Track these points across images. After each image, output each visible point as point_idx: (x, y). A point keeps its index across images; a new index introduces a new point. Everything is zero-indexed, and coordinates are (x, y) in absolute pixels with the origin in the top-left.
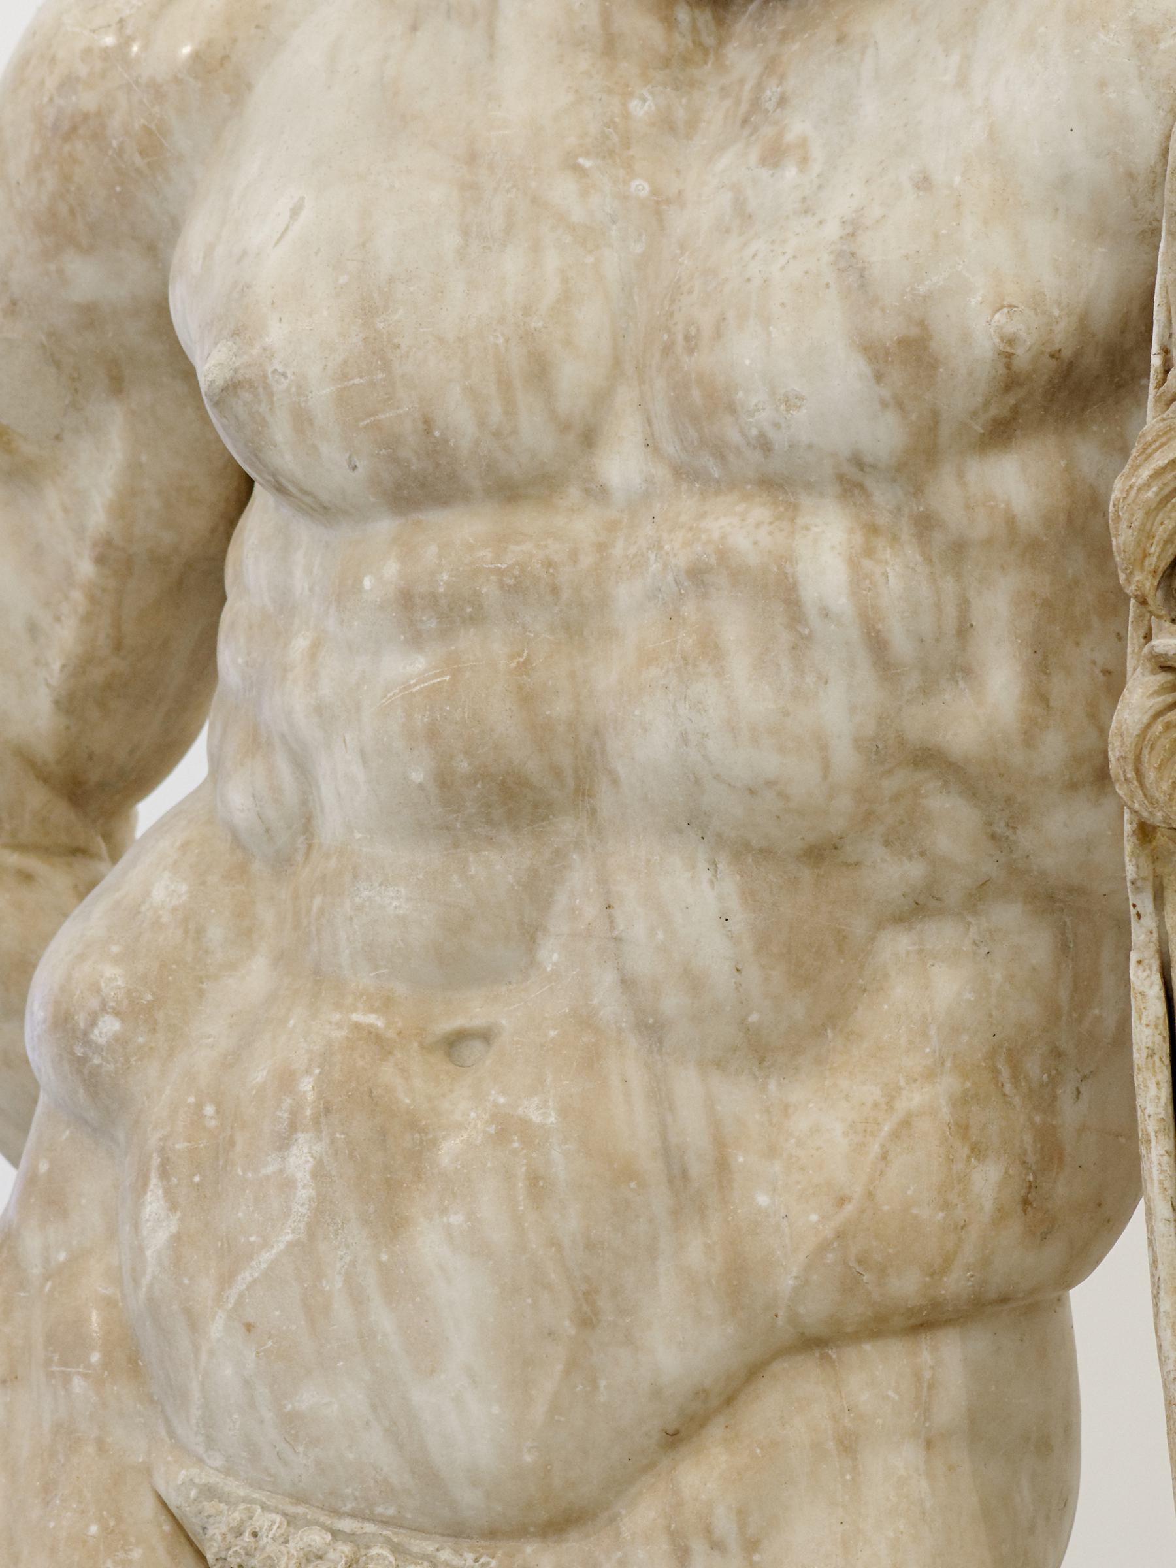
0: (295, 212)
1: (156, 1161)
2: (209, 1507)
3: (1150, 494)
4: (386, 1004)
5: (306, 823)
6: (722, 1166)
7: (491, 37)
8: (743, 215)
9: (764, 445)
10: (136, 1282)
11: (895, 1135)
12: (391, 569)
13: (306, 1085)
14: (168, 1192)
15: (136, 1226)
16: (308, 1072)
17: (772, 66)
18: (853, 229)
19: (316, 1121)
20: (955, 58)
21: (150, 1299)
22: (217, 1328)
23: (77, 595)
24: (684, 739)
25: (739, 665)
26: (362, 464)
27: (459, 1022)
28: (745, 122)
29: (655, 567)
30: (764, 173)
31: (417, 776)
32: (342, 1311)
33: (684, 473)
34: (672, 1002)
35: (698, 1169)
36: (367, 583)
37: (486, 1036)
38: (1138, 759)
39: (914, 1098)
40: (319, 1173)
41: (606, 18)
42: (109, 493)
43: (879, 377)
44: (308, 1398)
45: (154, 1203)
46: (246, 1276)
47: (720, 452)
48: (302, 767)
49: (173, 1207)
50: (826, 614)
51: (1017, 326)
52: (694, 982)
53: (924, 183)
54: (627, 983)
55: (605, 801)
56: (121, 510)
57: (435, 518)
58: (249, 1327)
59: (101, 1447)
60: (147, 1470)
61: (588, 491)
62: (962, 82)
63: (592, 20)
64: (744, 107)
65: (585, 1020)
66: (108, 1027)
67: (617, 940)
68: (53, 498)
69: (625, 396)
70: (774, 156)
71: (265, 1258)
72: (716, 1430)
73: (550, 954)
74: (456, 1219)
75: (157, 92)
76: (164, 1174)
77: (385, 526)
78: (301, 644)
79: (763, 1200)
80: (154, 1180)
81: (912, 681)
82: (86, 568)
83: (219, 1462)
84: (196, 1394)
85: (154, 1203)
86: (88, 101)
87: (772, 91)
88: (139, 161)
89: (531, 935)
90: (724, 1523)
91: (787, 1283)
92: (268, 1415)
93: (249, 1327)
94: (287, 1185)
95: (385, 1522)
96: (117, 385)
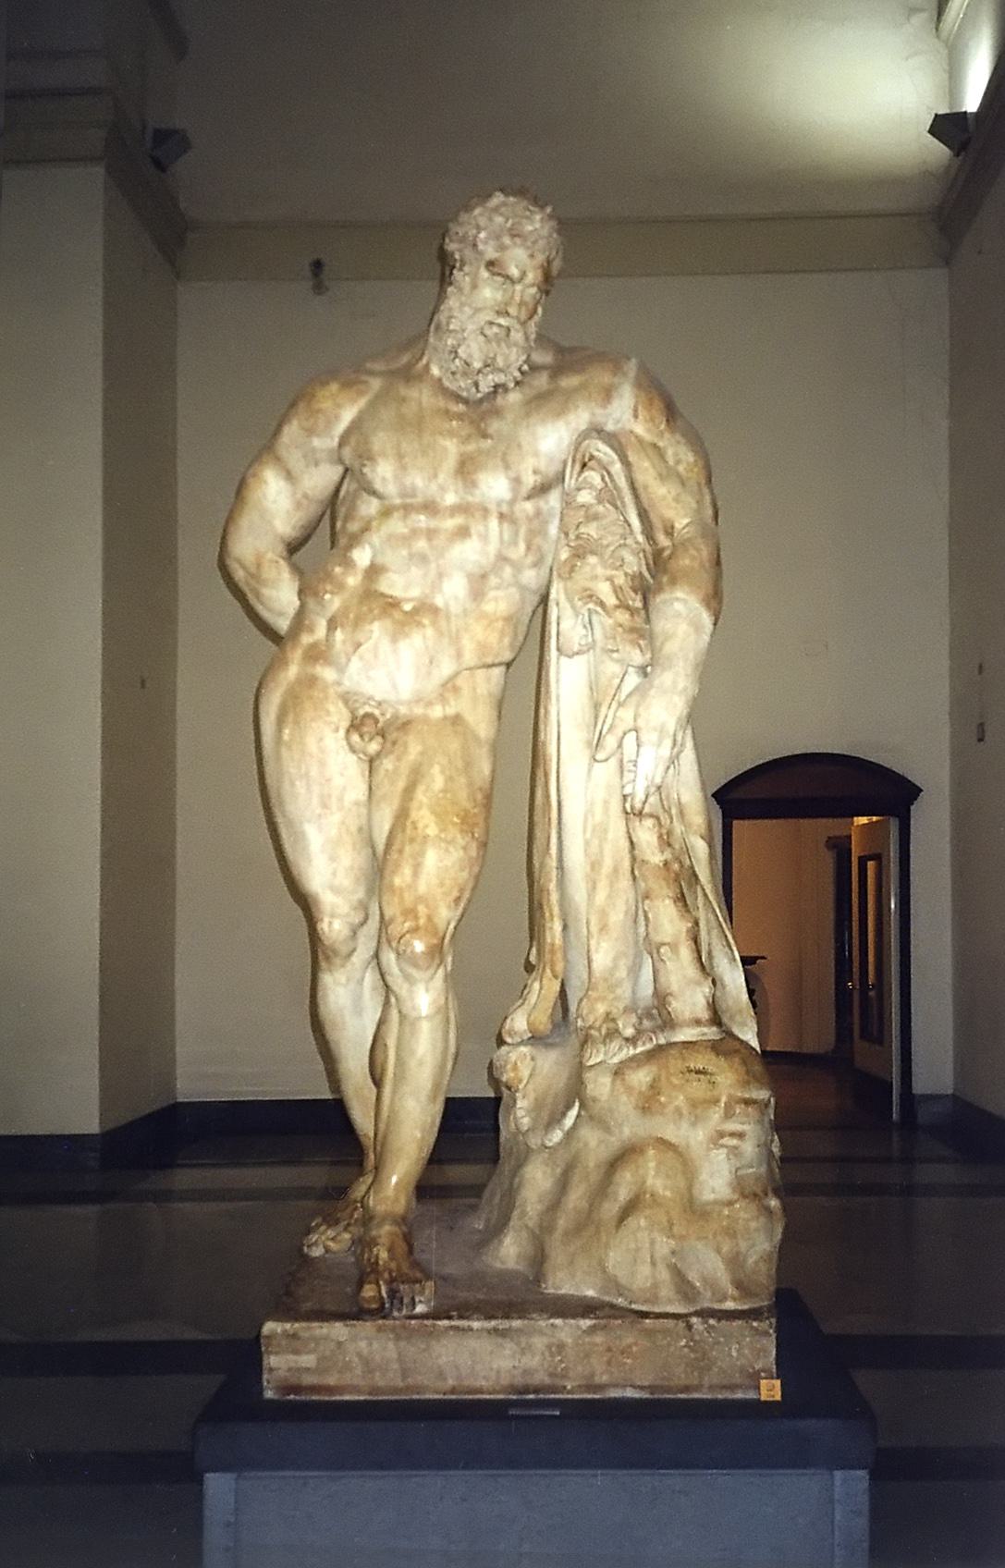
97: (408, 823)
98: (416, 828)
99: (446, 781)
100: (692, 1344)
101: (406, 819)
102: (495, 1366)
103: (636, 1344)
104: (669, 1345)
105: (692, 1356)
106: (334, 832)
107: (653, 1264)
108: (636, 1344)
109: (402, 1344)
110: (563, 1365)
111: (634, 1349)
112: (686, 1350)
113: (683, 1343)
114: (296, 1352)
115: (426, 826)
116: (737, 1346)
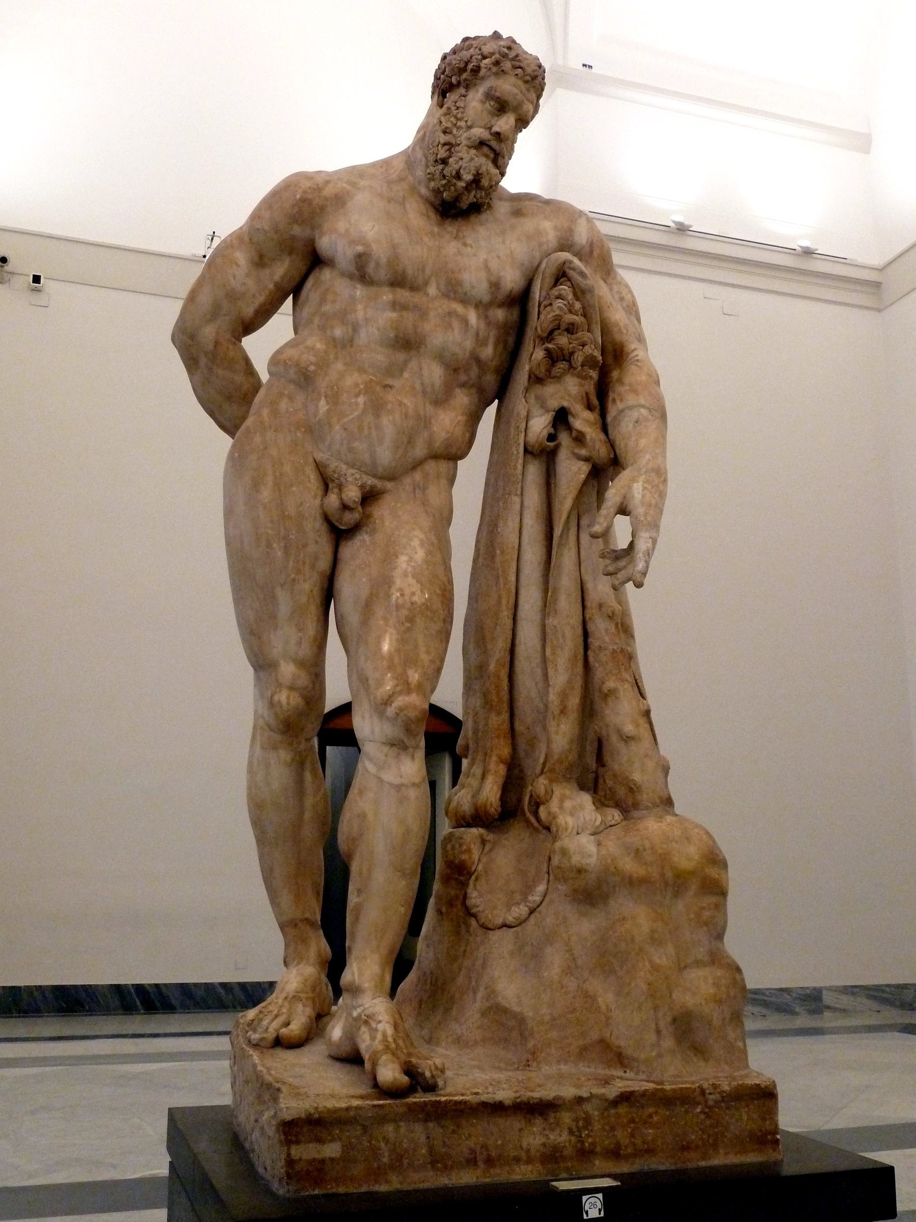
0: (373, 226)
1: (323, 394)
2: (330, 461)
3: (551, 319)
4: (375, 376)
5: (351, 340)
6: (430, 420)
7: (404, 208)
8: (459, 253)
9: (466, 294)
10: (315, 416)
11: (457, 423)
12: (391, 296)
13: (362, 386)
14: (327, 401)
15: (317, 406)
16: (362, 384)
17: (458, 231)
18: (486, 261)
19: (365, 393)
20: (501, 238)
21: (319, 420)
22: (337, 428)
23: (267, 292)
24: (444, 342)
25: (456, 331)
26: (388, 275)
27: (388, 383)
28: (455, 238)
29: (440, 310)
30: (463, 247)
31: (392, 335)
32: (366, 432)
33: (446, 296)
34: (429, 390)
35: (428, 420)
36: (384, 298)
37: (391, 387)
38: (539, 364)
39: (460, 418)
40: (365, 403)
41: (427, 212)
42: (282, 274)
43: (491, 287)
44: (356, 444)
45: (323, 402)
46: (346, 420)
47: (455, 292)
48: (355, 328)
49: (328, 403)
50: (472, 327)
51: (515, 286)
52: (433, 385)
53: (499, 257)
54: (422, 384)
55: (422, 350)
56: (282, 278)
57: (398, 290)
58: (345, 429)
59: (303, 446)
60: (312, 453)
61: (425, 293)
62: (504, 243)
63: (425, 211)
64: (454, 236)
65: (413, 388)
66: (312, 368)
67: (422, 375)
68: (267, 271)
69: (433, 279)
70: (465, 245)
71: (351, 417)
72: (419, 468)
73: (406, 375)
74: (391, 418)
75: (326, 199)
76: (326, 397)
77: (386, 289)
78: (360, 307)
79: (435, 429)
80: (323, 398)
81: (480, 342)
82: (271, 286)
83: (330, 454)
84: (329, 438)
85: (323, 402)
86: (310, 196)
87: (461, 235)
88: (318, 210)
89: (402, 371)
90: (421, 486)
91: (437, 444)
92: (345, 446)
93: (345, 429)
94: (357, 404)
95: (363, 471)
96: (290, 254)
97: (393, 590)
98: (402, 595)
99: (427, 556)
100: (707, 1110)
101: (390, 587)
102: (525, 1145)
103: (656, 1113)
104: (687, 1112)
105: (708, 1122)
106: (304, 599)
107: (658, 1032)
108: (656, 1113)
109: (431, 1125)
110: (590, 1140)
111: (655, 1119)
112: (702, 1117)
113: (698, 1110)
114: (320, 1141)
115: (413, 594)
116: (746, 1110)
